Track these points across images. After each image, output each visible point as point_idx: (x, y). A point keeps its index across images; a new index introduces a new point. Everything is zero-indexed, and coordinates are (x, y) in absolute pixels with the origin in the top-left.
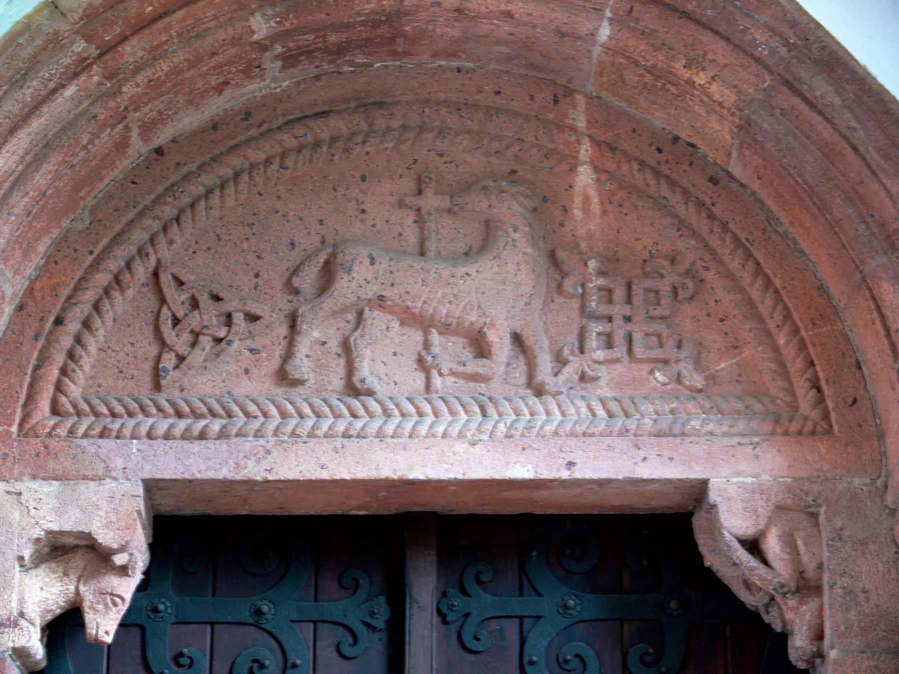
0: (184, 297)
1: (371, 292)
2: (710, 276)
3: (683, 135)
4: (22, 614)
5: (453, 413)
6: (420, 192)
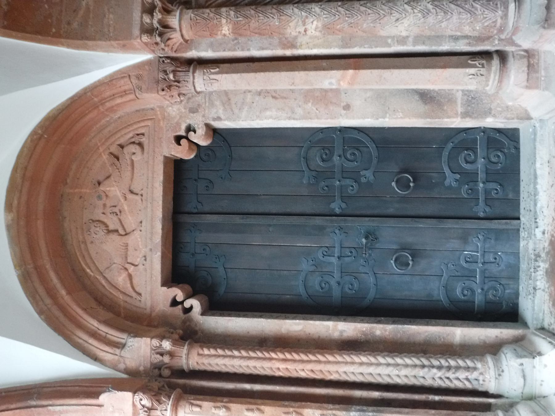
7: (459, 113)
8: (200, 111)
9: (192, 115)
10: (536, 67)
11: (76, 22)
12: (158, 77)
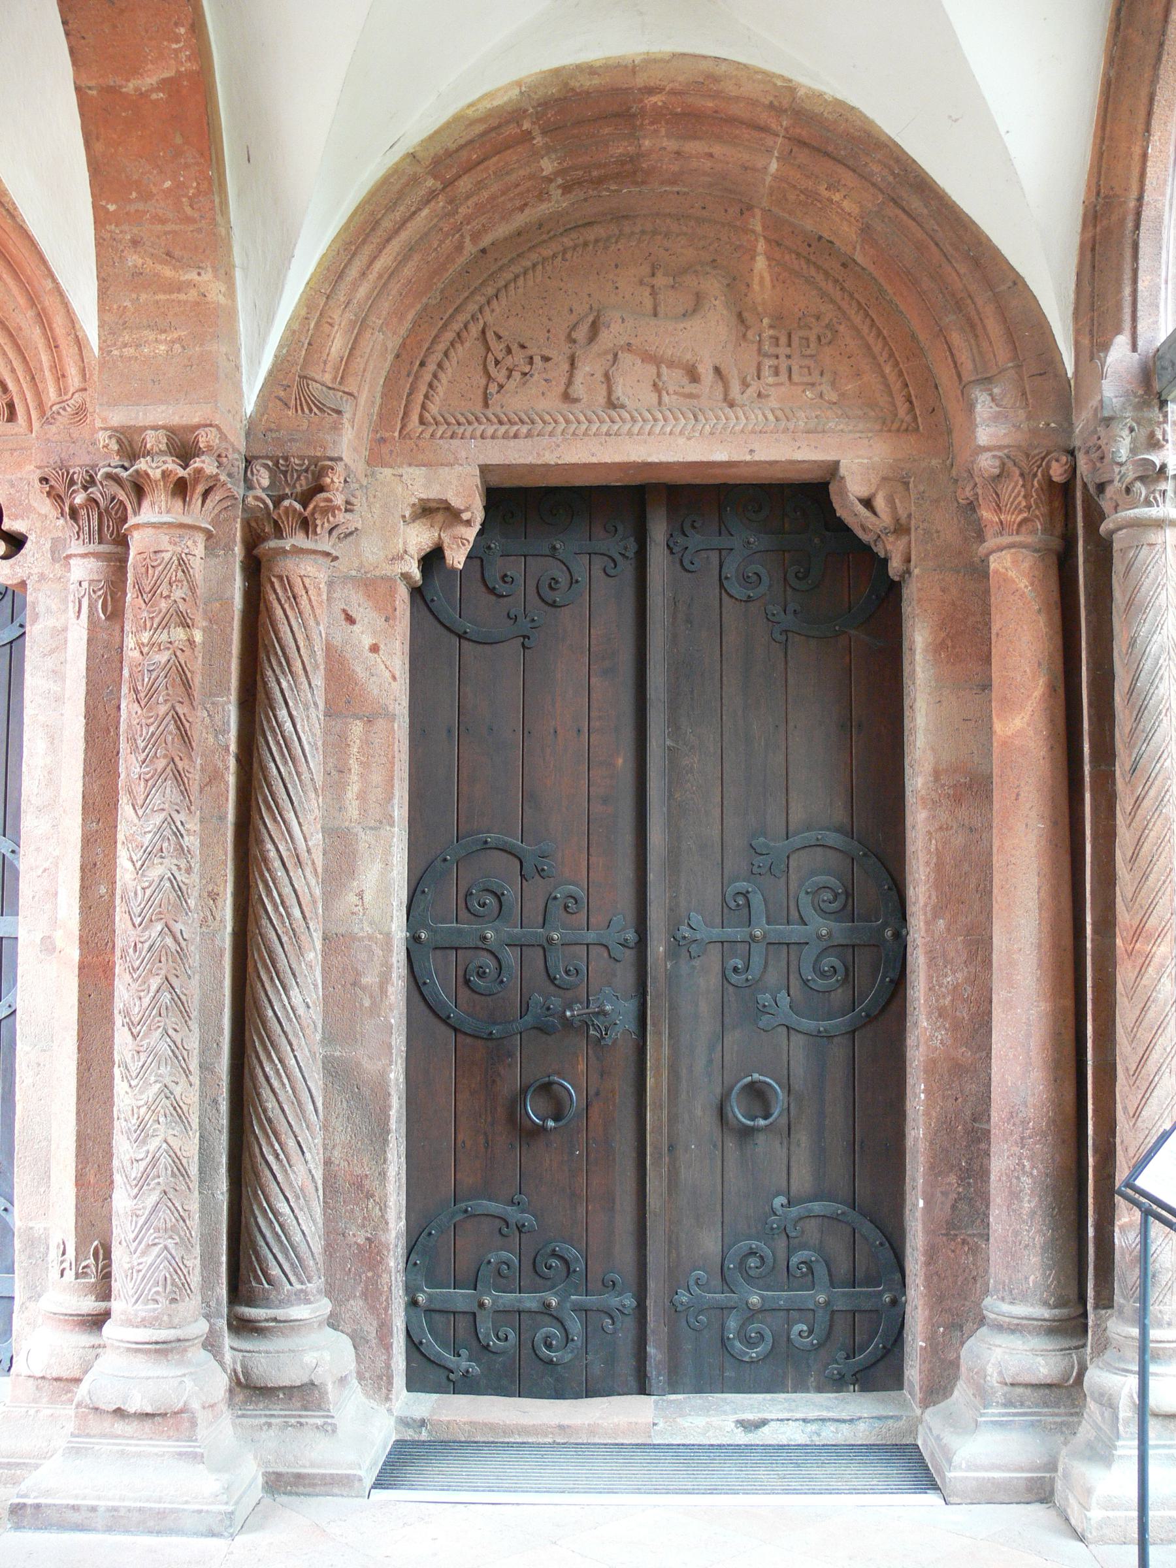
0: (502, 346)
1: (622, 341)
2: (841, 328)
3: (825, 235)
4: (406, 552)
5: (676, 419)
6: (653, 275)
7: (30, 1224)
9: (48, 546)
10: (64, 1398)
11: (140, 261)
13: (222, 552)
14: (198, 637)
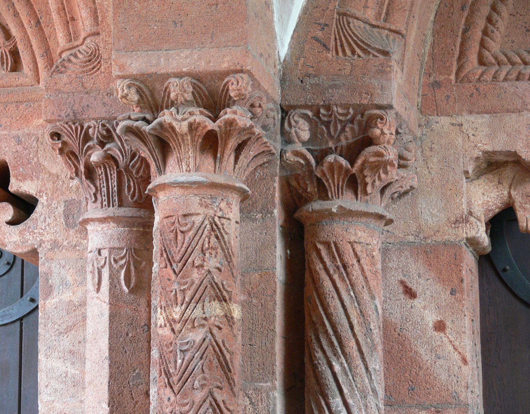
4: (471, 213)
8: (72, 232)
12: (90, 120)
13: (259, 216)
14: (237, 313)
